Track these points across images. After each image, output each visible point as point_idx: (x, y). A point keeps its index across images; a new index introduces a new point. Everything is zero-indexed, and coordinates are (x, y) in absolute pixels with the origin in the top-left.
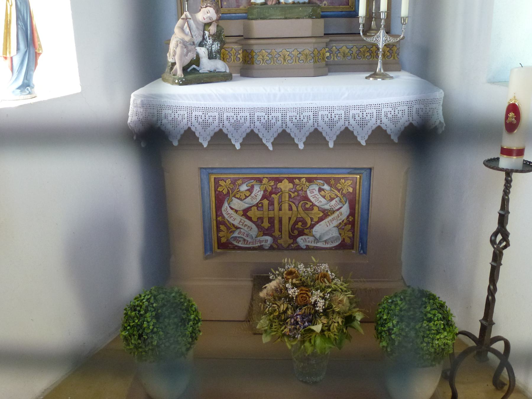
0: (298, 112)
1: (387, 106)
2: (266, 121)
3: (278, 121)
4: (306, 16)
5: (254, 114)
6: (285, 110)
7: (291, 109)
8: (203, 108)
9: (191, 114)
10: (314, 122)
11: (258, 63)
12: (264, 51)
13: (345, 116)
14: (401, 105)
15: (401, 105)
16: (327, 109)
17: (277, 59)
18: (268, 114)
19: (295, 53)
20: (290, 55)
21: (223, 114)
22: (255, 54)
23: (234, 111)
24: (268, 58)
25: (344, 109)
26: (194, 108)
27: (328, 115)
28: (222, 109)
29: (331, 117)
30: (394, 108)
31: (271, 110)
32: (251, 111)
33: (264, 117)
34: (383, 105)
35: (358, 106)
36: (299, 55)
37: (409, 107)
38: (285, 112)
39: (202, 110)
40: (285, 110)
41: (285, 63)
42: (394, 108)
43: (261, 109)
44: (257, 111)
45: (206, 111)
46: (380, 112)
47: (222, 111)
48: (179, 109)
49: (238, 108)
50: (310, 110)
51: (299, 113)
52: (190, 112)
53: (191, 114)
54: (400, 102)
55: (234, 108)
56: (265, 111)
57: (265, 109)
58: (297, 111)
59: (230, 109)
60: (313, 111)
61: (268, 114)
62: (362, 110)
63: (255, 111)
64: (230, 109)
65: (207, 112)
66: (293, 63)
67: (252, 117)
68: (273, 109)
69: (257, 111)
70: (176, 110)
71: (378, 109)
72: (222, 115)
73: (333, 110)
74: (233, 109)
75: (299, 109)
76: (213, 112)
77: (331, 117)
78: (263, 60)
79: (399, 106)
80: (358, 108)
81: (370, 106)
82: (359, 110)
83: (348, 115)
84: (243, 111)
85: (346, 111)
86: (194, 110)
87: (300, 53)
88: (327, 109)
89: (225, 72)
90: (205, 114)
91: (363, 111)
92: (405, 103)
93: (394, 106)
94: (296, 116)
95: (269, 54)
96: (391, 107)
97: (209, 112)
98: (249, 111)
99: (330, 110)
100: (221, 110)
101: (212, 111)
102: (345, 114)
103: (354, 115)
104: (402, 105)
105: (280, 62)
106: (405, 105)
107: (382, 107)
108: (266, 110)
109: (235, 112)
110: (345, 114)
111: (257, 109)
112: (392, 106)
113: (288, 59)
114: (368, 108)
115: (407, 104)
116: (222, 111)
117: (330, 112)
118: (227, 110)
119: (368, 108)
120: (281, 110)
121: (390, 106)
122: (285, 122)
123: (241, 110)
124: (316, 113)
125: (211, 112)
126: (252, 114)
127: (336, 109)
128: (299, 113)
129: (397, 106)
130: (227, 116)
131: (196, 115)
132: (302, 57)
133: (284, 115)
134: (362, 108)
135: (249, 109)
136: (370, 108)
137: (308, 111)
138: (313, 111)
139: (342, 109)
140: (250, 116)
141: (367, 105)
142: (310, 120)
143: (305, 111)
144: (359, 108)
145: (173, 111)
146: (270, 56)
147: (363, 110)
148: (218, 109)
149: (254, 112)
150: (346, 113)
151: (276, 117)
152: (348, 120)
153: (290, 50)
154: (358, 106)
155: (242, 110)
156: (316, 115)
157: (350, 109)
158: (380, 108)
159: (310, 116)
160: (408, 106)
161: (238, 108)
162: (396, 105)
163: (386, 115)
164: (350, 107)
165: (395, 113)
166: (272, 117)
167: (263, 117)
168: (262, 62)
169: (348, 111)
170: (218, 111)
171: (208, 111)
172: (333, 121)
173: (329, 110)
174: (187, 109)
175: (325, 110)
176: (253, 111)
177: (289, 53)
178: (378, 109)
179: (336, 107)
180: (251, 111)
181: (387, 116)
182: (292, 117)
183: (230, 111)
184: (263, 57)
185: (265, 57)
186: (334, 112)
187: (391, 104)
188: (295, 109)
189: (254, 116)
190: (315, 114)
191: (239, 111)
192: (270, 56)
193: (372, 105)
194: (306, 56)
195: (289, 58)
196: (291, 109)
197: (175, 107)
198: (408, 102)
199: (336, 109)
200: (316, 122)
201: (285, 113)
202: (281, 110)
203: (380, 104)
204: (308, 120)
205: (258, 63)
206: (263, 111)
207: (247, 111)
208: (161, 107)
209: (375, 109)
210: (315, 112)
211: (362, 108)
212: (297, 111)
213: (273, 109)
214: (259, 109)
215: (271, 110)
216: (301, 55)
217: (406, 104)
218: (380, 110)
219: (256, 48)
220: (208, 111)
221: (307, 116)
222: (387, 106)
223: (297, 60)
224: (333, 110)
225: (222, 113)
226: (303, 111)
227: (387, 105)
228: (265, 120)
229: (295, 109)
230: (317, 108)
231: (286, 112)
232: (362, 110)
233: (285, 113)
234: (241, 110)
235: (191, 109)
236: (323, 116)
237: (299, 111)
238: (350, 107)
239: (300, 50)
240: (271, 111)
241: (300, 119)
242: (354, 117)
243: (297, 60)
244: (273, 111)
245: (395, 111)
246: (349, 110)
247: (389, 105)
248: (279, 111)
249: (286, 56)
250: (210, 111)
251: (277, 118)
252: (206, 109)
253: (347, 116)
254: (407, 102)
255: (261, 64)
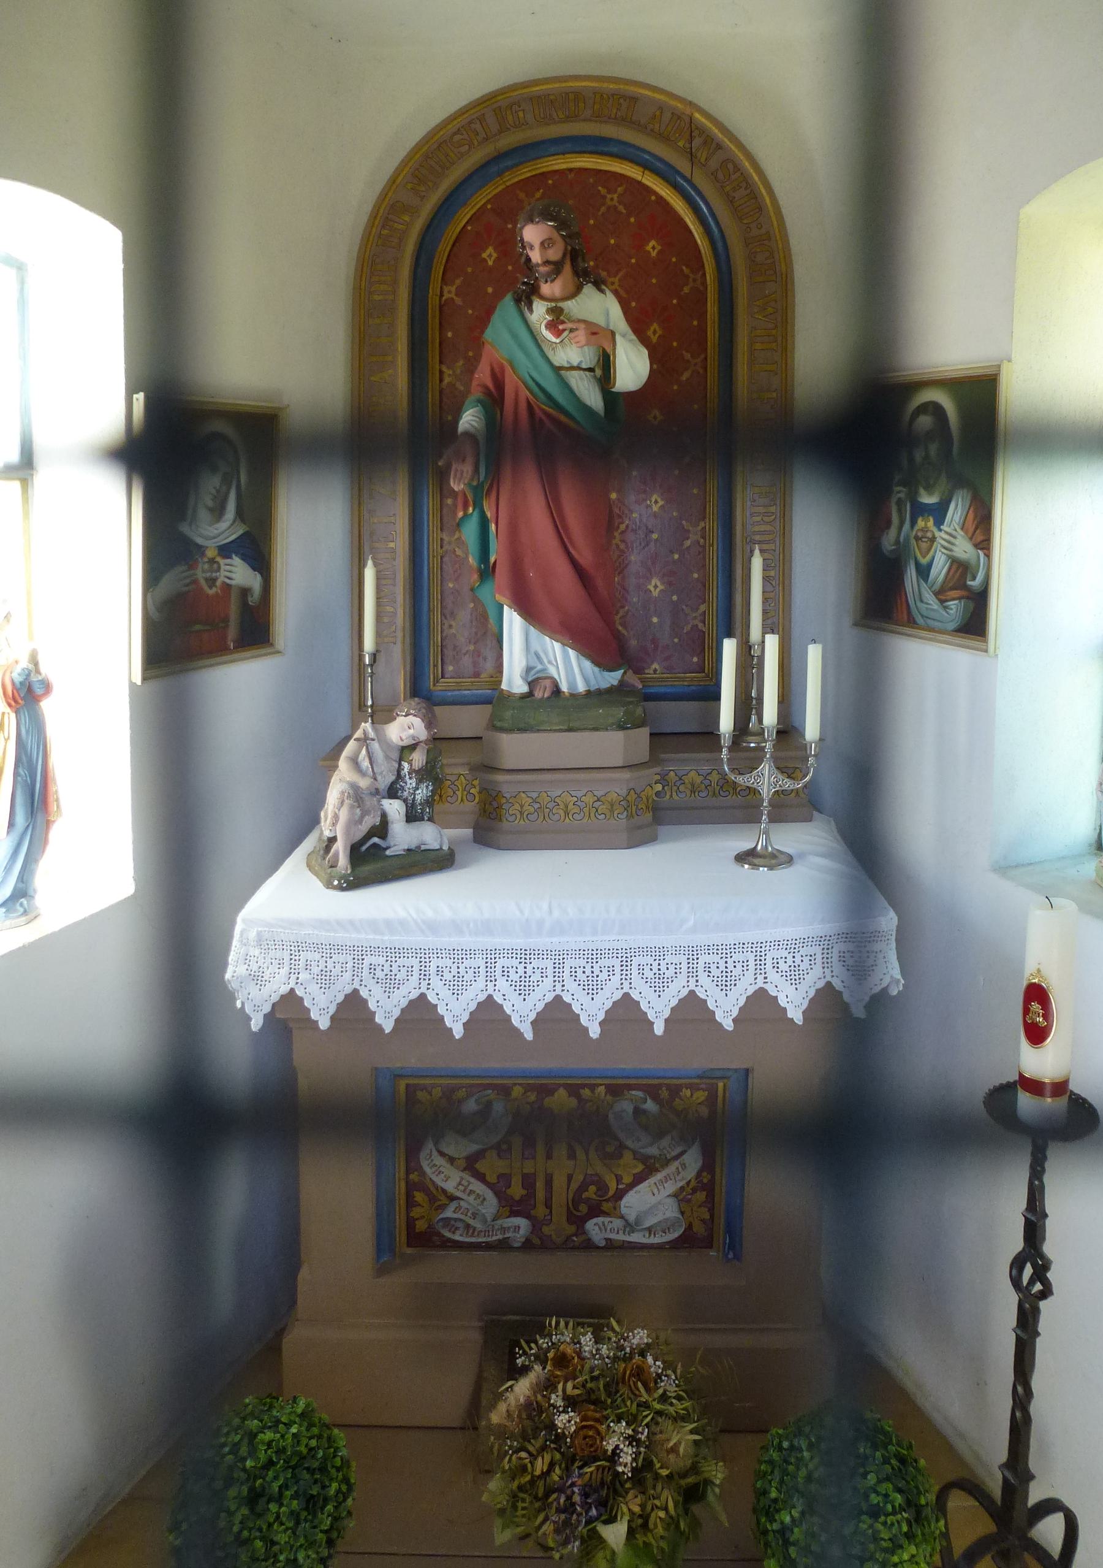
0: (588, 958)
1: (776, 947)
2: (521, 977)
3: (547, 976)
4: (613, 724)
5: (495, 963)
6: (561, 953)
7: (574, 952)
8: (386, 948)
9: (360, 962)
10: (622, 979)
11: (510, 819)
12: (523, 795)
13: (689, 968)
14: (806, 944)
15: (806, 944)
16: (649, 953)
17: (551, 810)
18: (525, 963)
19: (589, 799)
20: (579, 803)
21: (430, 962)
22: (504, 800)
23: (452, 956)
24: (532, 810)
25: (687, 953)
26: (368, 949)
27: (651, 965)
28: (427, 952)
29: (659, 970)
30: (792, 950)
31: (530, 954)
32: (489, 956)
33: (517, 968)
34: (768, 944)
35: (715, 947)
36: (597, 804)
37: (823, 949)
38: (561, 957)
39: (385, 954)
40: (561, 953)
41: (567, 820)
42: (792, 950)
43: (510, 952)
44: (501, 956)
45: (393, 955)
46: (763, 958)
47: (427, 956)
48: (336, 951)
49: (462, 950)
50: (615, 955)
51: (589, 960)
52: (360, 957)
53: (360, 962)
54: (804, 939)
55: (454, 950)
56: (519, 956)
57: (519, 952)
58: (586, 957)
59: (443, 952)
60: (619, 956)
61: (525, 963)
62: (724, 955)
63: (497, 955)
64: (443, 952)
65: (396, 957)
66: (585, 820)
67: (491, 968)
68: (536, 953)
69: (501, 956)
70: (331, 953)
71: (758, 953)
72: (428, 964)
73: (664, 955)
74: (452, 952)
75: (590, 952)
76: (408, 957)
77: (659, 970)
78: (521, 813)
79: (803, 947)
80: (715, 951)
81: (741, 945)
82: (717, 954)
83: (695, 966)
84: (472, 956)
85: (690, 956)
86: (368, 953)
87: (598, 800)
88: (649, 953)
89: (441, 849)
90: (391, 961)
91: (726, 958)
92: (814, 940)
93: (793, 946)
94: (584, 968)
95: (535, 801)
96: (786, 949)
97: (400, 957)
98: (485, 956)
99: (658, 953)
100: (425, 954)
101: (406, 955)
102: (689, 963)
103: (707, 965)
104: (810, 944)
105: (556, 817)
106: (814, 943)
107: (768, 948)
108: (521, 954)
109: (454, 958)
110: (689, 963)
111: (502, 952)
112: (788, 947)
113: (573, 812)
114: (737, 951)
115: (820, 941)
116: (427, 956)
117: (657, 957)
118: (437, 953)
119: (737, 951)
120: (553, 953)
121: (785, 947)
122: (561, 979)
123: (468, 953)
124: (627, 961)
125: (404, 957)
126: (491, 963)
127: (670, 953)
128: (589, 960)
129: (798, 945)
130: (438, 967)
131: (371, 965)
132: (603, 808)
133: (559, 964)
134: (724, 951)
135: (484, 952)
136: (741, 949)
137: (610, 956)
138: (619, 956)
139: (682, 952)
140: (487, 967)
141: (735, 944)
142: (613, 975)
143: (603, 956)
144: (718, 950)
145: (324, 955)
146: (537, 806)
147: (727, 954)
148: (418, 951)
149: (495, 958)
150: (691, 961)
151: (542, 969)
152: (694, 975)
153: (579, 794)
154: (715, 947)
155: (470, 954)
156: (627, 966)
157: (699, 952)
158: (763, 950)
159: (613, 966)
160: (822, 947)
161: (462, 950)
162: (796, 944)
163: (775, 964)
164: (699, 948)
165: (794, 962)
166: (534, 968)
167: (514, 968)
168: (519, 816)
169: (695, 957)
170: (419, 956)
171: (397, 954)
172: (664, 978)
173: (653, 954)
174: (354, 950)
175: (645, 954)
176: (493, 956)
177: (576, 799)
178: (758, 953)
179: (670, 949)
180: (489, 956)
181: (778, 968)
182: (575, 968)
183: (444, 956)
184: (522, 806)
185: (526, 807)
186: (664, 959)
187: (786, 942)
188: (581, 952)
189: (495, 967)
190: (624, 963)
191: (464, 956)
192: (537, 806)
193: (746, 944)
194: (612, 805)
195: (577, 810)
196: (574, 952)
197: (328, 947)
198: (821, 937)
199: (670, 953)
200: (626, 979)
201: (561, 961)
202: (553, 953)
203: (762, 943)
204: (609, 976)
205: (510, 819)
206: (514, 955)
207: (480, 956)
208: (298, 946)
209: (752, 952)
210: (624, 958)
211: (724, 951)
212: (586, 957)
213: (536, 953)
214: (506, 951)
215: (530, 954)
216: (600, 803)
217: (818, 943)
218: (763, 954)
219: (507, 791)
220: (397, 954)
221: (609, 967)
222: (776, 947)
223: (592, 815)
224: (664, 955)
225: (427, 960)
226: (599, 956)
227: (777, 943)
228: (519, 975)
229: (581, 952)
230: (628, 951)
231: (563, 959)
232: (724, 955)
233: (561, 961)
234: (468, 953)
235: (362, 951)
236: (641, 967)
237: (590, 956)
238: (699, 948)
239: (599, 794)
240: (532, 956)
241: (593, 972)
242: (707, 969)
243: (592, 815)
244: (536, 957)
245: (794, 957)
246: (697, 954)
247: (781, 943)
248: (549, 956)
249: (571, 806)
250: (402, 955)
251: (544, 971)
252: (393, 951)
253: (693, 968)
254: (819, 939)
255: (516, 822)
